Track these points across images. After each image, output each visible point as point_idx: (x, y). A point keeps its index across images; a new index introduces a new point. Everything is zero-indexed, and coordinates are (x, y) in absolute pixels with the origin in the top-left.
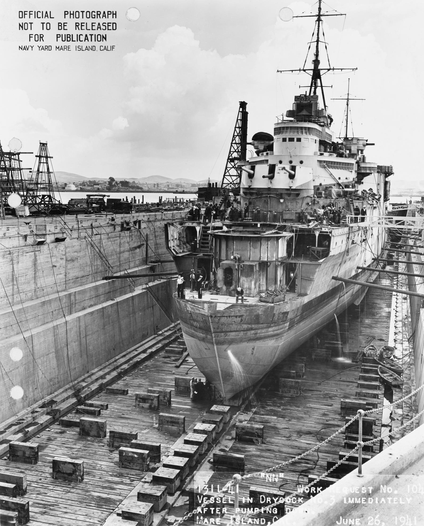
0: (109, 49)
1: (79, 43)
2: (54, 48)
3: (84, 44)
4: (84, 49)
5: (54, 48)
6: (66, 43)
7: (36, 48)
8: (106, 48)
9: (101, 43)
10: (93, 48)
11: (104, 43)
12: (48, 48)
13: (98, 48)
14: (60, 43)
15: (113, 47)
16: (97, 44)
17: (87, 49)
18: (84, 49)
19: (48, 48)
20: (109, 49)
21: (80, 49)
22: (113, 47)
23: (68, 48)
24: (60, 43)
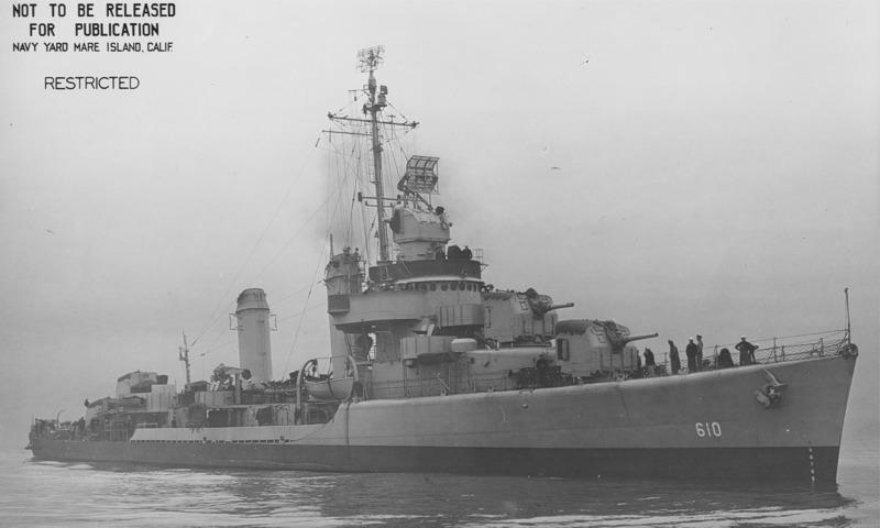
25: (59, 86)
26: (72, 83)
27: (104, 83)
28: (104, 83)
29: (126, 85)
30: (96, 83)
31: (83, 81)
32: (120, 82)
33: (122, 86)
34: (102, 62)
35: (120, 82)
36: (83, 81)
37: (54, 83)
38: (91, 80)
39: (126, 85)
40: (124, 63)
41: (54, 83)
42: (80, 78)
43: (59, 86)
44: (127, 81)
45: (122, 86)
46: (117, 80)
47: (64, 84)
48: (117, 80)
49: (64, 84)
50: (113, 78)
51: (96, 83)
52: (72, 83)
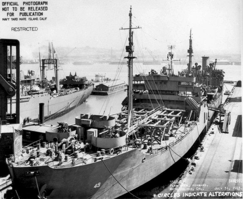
0: (44, 19)
1: (30, 17)
2: (19, 19)
3: (33, 17)
4: (32, 19)
5: (19, 19)
6: (24, 17)
8: (42, 19)
10: (36, 19)
11: (42, 17)
12: (16, 19)
13: (39, 19)
14: (22, 17)
15: (46, 18)
16: (39, 17)
17: (34, 19)
18: (32, 19)
19: (16, 19)
20: (44, 19)
21: (30, 19)
22: (46, 18)
23: (25, 19)
24: (22, 17)
28: (28, 29)
31: (22, 29)
32: (32, 29)
33: (33, 30)
34: (27, 23)
35: (32, 29)
36: (22, 29)
38: (24, 28)
39: (34, 29)
42: (21, 28)
45: (33, 30)
46: (31, 28)
47: (17, 29)
48: (31, 28)
49: (17, 29)
50: (30, 28)
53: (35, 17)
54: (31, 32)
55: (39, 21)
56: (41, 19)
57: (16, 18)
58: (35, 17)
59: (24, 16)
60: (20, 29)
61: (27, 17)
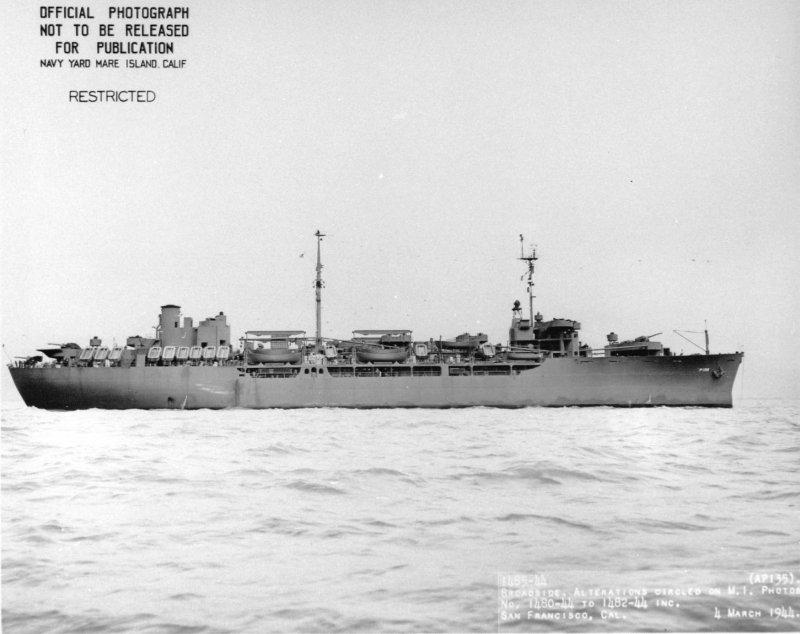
0: (177, 65)
2: (93, 63)
3: (140, 58)
4: (139, 64)
5: (93, 63)
6: (112, 56)
7: (66, 64)
8: (172, 64)
9: (166, 56)
10: (152, 64)
11: (169, 56)
12: (84, 63)
13: (160, 63)
14: (103, 56)
15: (182, 63)
16: (159, 58)
17: (144, 64)
18: (139, 64)
19: (84, 63)
20: (177, 65)
21: (133, 64)
22: (182, 63)
23: (114, 63)
25: (82, 99)
26: (94, 96)
27: (123, 96)
28: (123, 96)
29: (144, 98)
30: (116, 96)
31: (104, 95)
32: (138, 95)
33: (140, 99)
34: (120, 77)
35: (138, 95)
36: (104, 95)
37: (78, 96)
38: (111, 94)
39: (144, 98)
40: (141, 79)
41: (78, 96)
43: (82, 99)
44: (144, 94)
45: (140, 99)
46: (135, 94)
48: (135, 94)
49: (87, 97)
51: (116, 96)
52: (94, 96)
53: (147, 57)
54: (132, 105)
55: (160, 72)
56: (167, 64)
57: (84, 58)
58: (147, 57)
59: (112, 53)
60: (98, 95)
61: (122, 58)
